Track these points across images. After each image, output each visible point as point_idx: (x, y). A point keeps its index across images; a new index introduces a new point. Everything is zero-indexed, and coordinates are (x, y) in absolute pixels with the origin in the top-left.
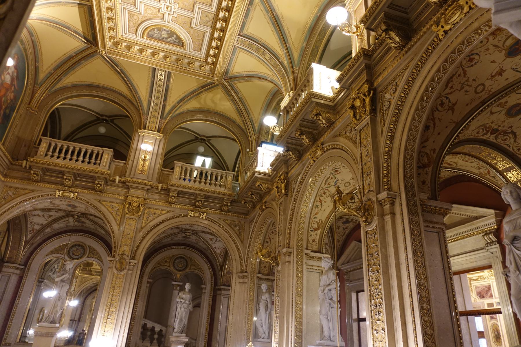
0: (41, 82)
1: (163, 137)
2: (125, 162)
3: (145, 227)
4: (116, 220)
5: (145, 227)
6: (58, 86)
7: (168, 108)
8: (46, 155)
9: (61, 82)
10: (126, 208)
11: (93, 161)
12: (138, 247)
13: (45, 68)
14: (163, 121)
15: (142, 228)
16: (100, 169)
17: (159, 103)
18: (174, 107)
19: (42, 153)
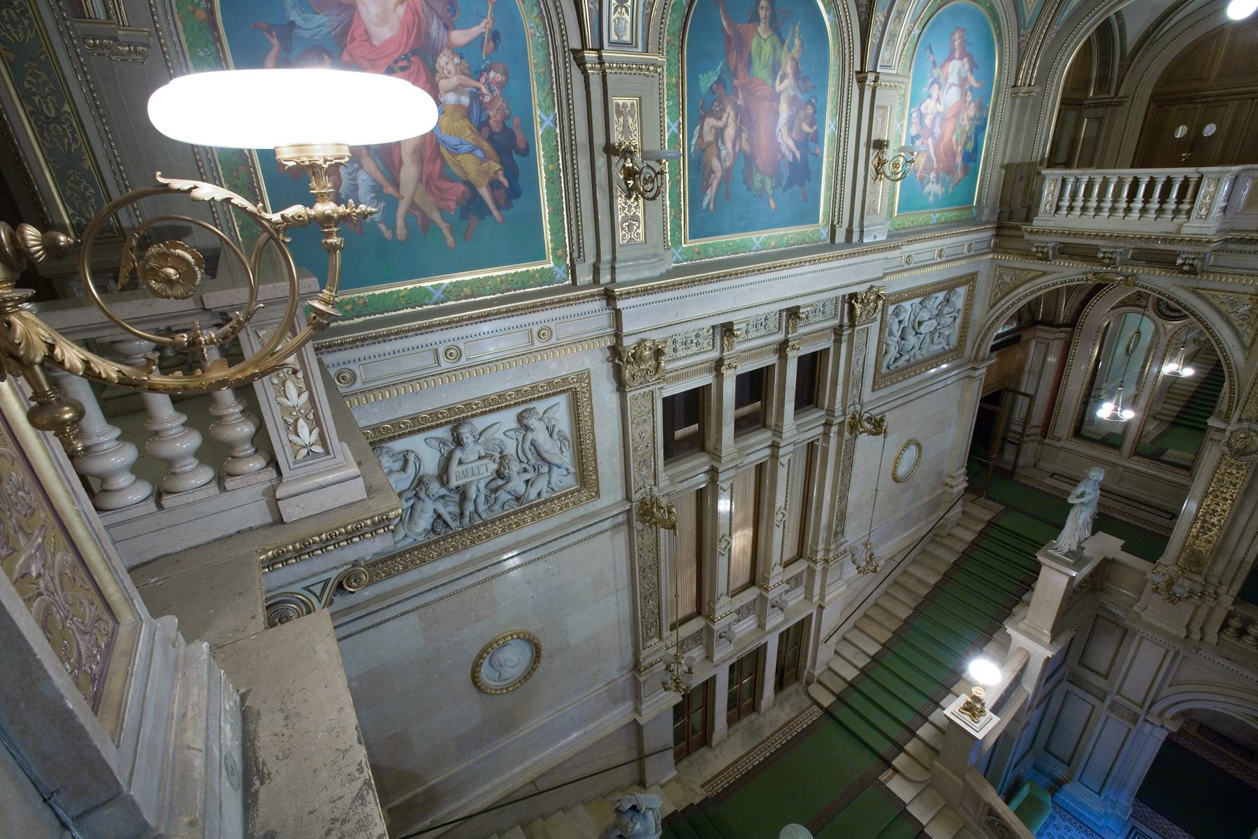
0: (1031, 21)
8: (1058, 208)
19: (1048, 207)
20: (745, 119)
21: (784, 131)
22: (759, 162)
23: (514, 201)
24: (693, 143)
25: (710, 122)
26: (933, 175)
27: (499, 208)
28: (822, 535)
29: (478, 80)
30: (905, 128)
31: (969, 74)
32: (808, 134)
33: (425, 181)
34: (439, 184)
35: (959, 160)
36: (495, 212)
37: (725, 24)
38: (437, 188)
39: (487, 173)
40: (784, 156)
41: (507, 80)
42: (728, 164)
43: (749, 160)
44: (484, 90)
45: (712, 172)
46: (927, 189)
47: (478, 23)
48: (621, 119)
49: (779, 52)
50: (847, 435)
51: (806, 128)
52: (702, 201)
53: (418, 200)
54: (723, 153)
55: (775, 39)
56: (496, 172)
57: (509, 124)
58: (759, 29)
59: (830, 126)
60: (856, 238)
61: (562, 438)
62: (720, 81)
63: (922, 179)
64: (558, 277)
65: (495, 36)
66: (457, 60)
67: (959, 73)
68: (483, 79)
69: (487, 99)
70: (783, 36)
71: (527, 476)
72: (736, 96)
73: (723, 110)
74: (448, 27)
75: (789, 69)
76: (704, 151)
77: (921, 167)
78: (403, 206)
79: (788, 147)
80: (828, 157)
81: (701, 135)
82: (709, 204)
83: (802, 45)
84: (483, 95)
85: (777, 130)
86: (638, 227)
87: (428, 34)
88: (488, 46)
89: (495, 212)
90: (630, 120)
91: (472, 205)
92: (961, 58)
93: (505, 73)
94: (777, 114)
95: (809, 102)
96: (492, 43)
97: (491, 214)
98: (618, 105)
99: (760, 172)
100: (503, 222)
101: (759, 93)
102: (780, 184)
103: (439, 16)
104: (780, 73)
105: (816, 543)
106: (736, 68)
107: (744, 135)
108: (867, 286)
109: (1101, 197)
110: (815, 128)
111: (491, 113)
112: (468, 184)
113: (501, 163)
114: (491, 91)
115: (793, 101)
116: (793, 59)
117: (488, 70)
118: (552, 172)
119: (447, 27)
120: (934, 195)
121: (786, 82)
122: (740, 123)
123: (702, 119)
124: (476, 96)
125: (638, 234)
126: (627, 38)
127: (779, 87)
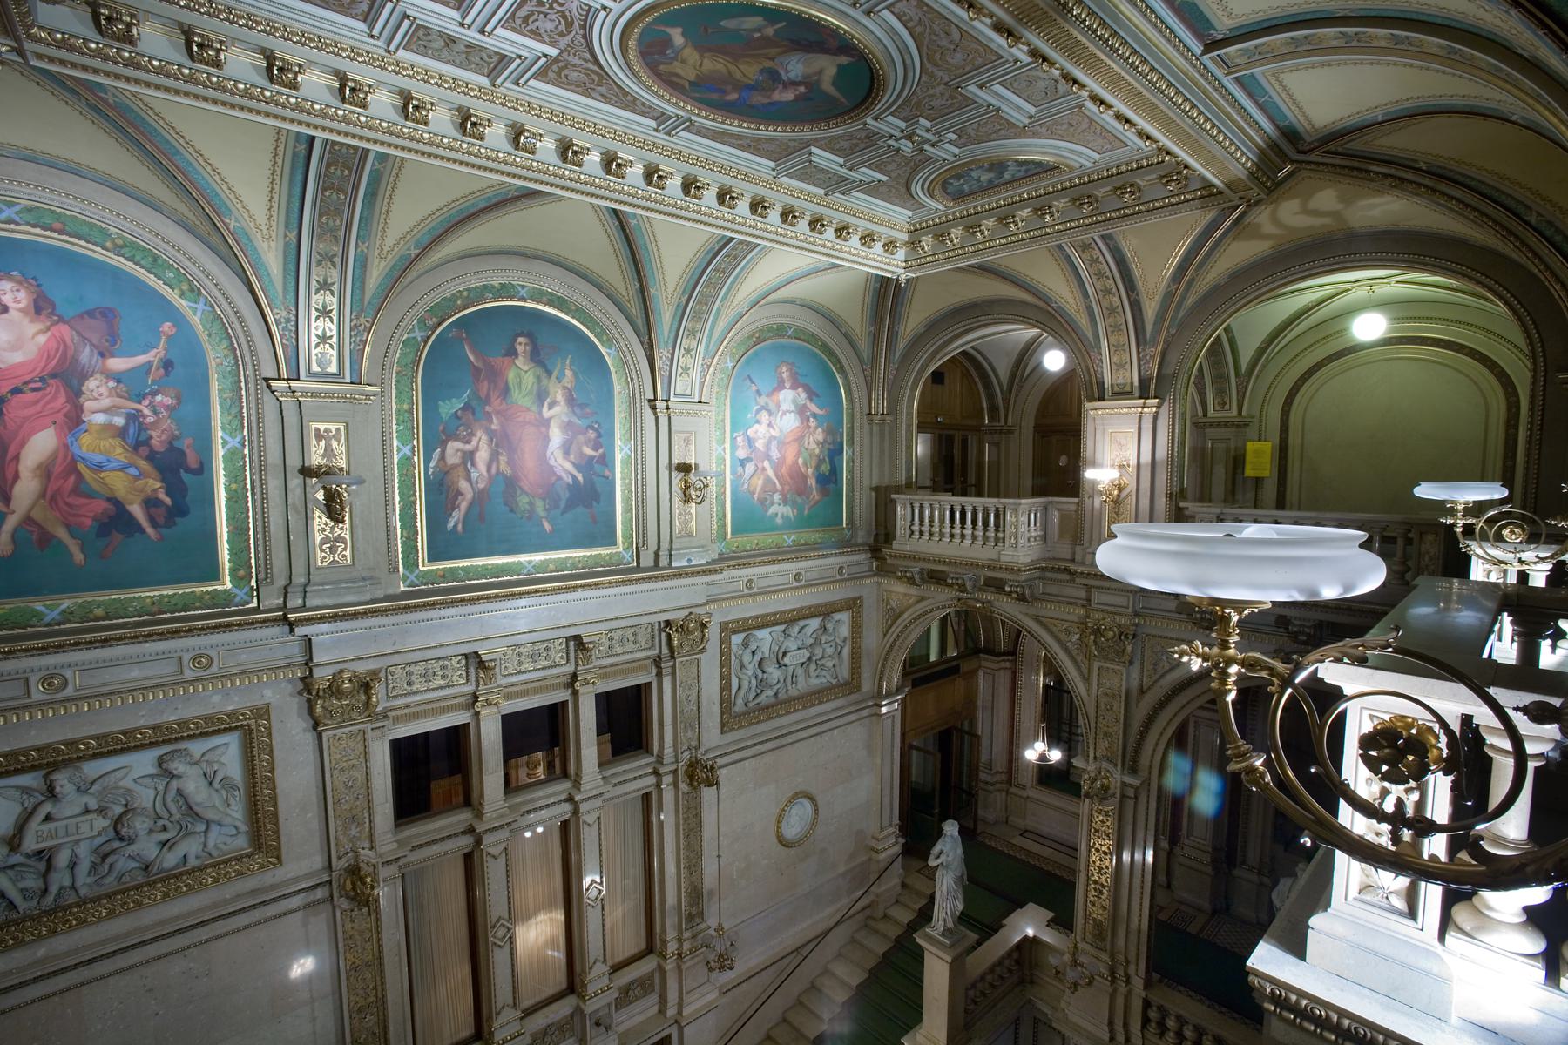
1: (1159, 406)
2: (1076, 500)
3: (1149, 688)
4: (1078, 668)
5: (1149, 688)
6: (901, 345)
7: (1150, 309)
9: (901, 336)
10: (1091, 643)
11: (991, 534)
12: (1140, 742)
13: (858, 331)
14: (1150, 351)
15: (1142, 692)
16: (1007, 555)
17: (1119, 303)
18: (1168, 296)
20: (501, 442)
21: (559, 455)
22: (525, 485)
23: (178, 520)
24: (432, 465)
25: (453, 446)
26: (777, 497)
27: (154, 523)
28: (671, 921)
29: (140, 403)
30: (728, 451)
31: (808, 402)
32: (592, 458)
34: (69, 500)
35: (812, 482)
36: (150, 530)
37: (471, 357)
38: (67, 504)
39: (142, 491)
40: (560, 478)
41: (179, 404)
42: (481, 486)
43: (511, 484)
44: (146, 411)
45: (459, 493)
46: (772, 510)
47: (145, 352)
48: (322, 443)
49: (545, 381)
50: (684, 787)
51: (588, 451)
52: (446, 522)
54: (474, 475)
55: (539, 371)
56: (155, 490)
57: (176, 444)
58: (517, 362)
59: (622, 450)
60: (664, 562)
61: (228, 784)
62: (466, 408)
63: (762, 501)
64: (238, 599)
65: (167, 365)
66: (112, 384)
67: (794, 401)
68: (146, 402)
69: (150, 420)
70: (549, 367)
71: (164, 836)
72: (491, 421)
73: (473, 434)
75: (560, 397)
76: (447, 473)
77: (758, 489)
79: (565, 470)
80: (622, 479)
81: (442, 457)
82: (455, 526)
83: (575, 374)
84: (145, 417)
85: (549, 453)
86: (345, 549)
87: (75, 360)
88: (158, 373)
89: (150, 530)
90: (334, 444)
91: (117, 520)
92: (792, 388)
93: (178, 398)
94: (547, 439)
95: (590, 427)
96: (162, 371)
97: (142, 531)
98: (317, 430)
99: (527, 493)
100: (162, 538)
101: (520, 419)
102: (557, 506)
103: (92, 344)
104: (548, 400)
105: (664, 931)
106: (488, 396)
107: (503, 459)
108: (686, 612)
109: (974, 522)
110: (601, 451)
111: (154, 434)
113: (163, 481)
114: (156, 413)
115: (567, 427)
116: (565, 388)
117: (154, 394)
118: (236, 491)
119: (102, 355)
120: (783, 517)
121: (557, 409)
122: (497, 445)
123: (444, 444)
124: (134, 417)
125: (344, 556)
126: (333, 369)
127: (546, 413)
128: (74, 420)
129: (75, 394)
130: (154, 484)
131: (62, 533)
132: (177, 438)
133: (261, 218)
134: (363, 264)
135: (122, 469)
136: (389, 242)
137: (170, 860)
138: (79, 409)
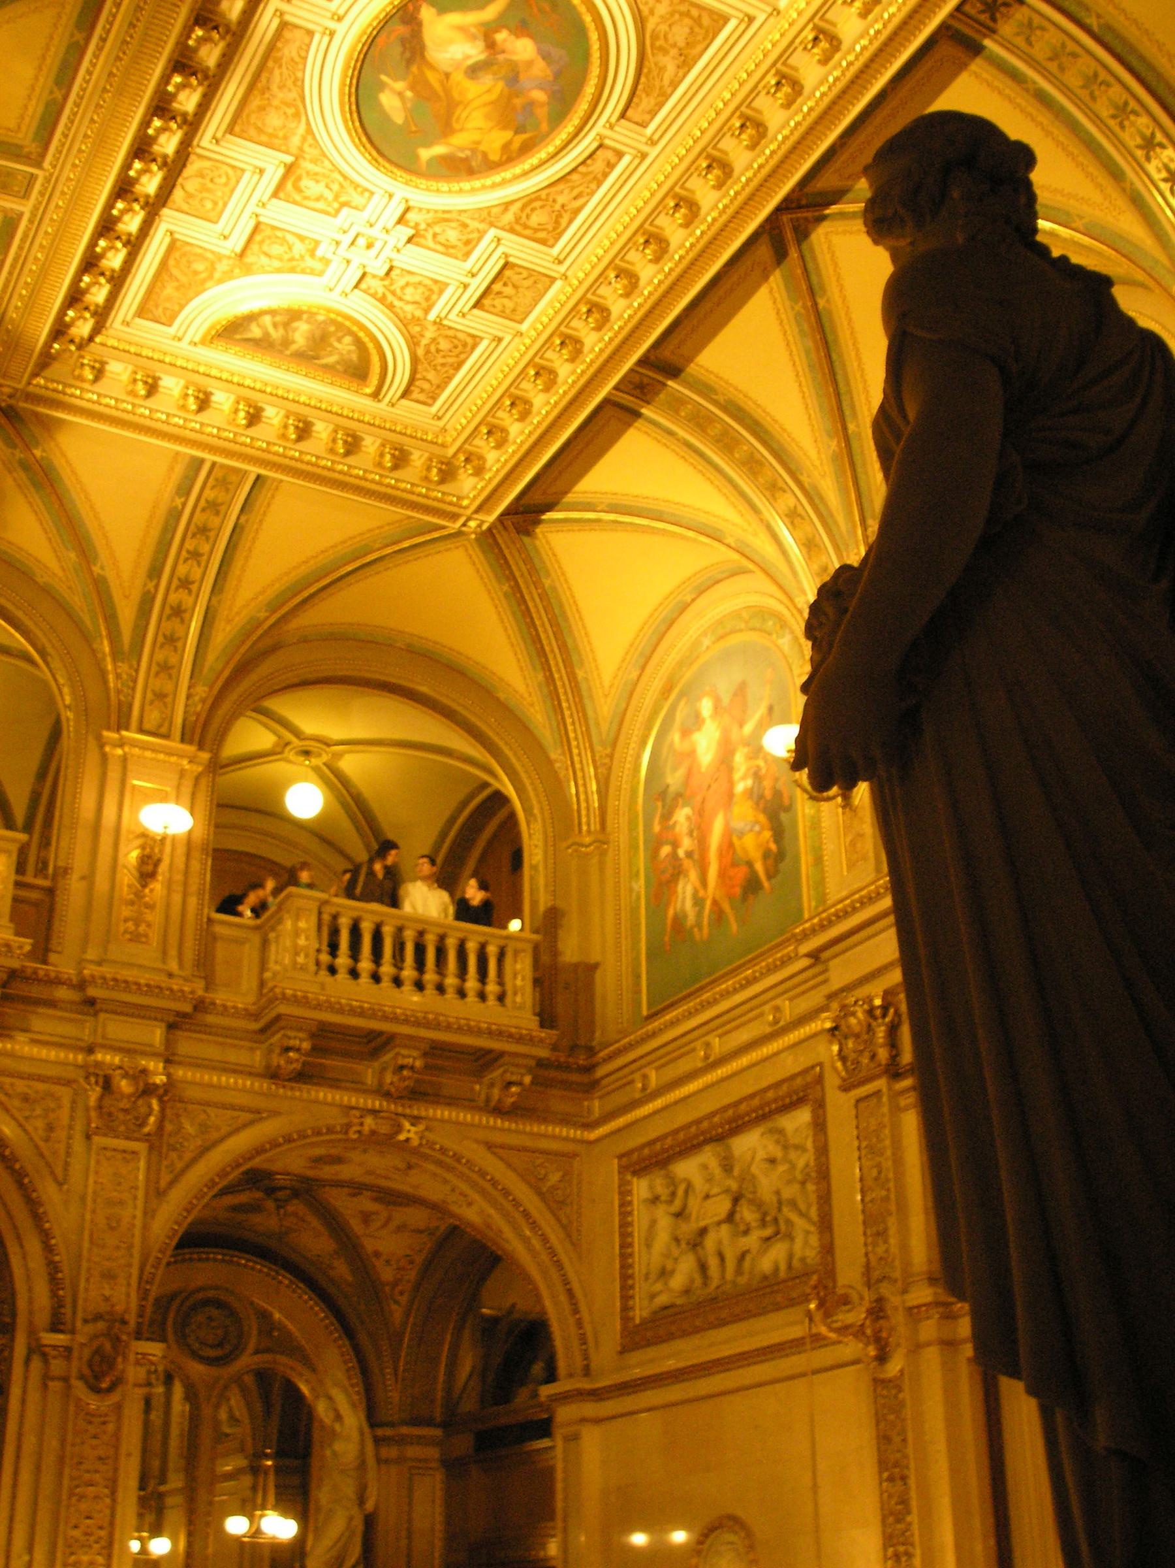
27: (770, 877)
33: (722, 874)
36: (766, 884)
44: (761, 763)
53: (717, 898)
57: (778, 787)
66: (746, 750)
74: (741, 725)
78: (708, 903)
112: (750, 864)
124: (757, 776)
128: (730, 795)
129: (730, 770)
130: (767, 834)
131: (726, 906)
132: (776, 780)
133: (738, 519)
134: (813, 496)
135: (751, 830)
136: (813, 453)
137: (766, 1264)
138: (731, 784)
